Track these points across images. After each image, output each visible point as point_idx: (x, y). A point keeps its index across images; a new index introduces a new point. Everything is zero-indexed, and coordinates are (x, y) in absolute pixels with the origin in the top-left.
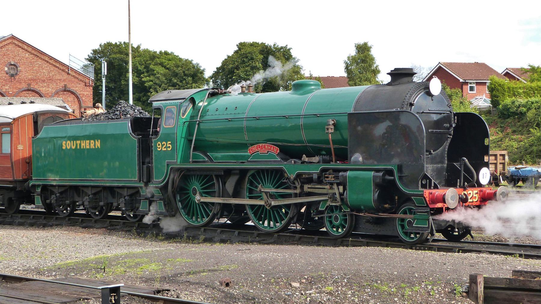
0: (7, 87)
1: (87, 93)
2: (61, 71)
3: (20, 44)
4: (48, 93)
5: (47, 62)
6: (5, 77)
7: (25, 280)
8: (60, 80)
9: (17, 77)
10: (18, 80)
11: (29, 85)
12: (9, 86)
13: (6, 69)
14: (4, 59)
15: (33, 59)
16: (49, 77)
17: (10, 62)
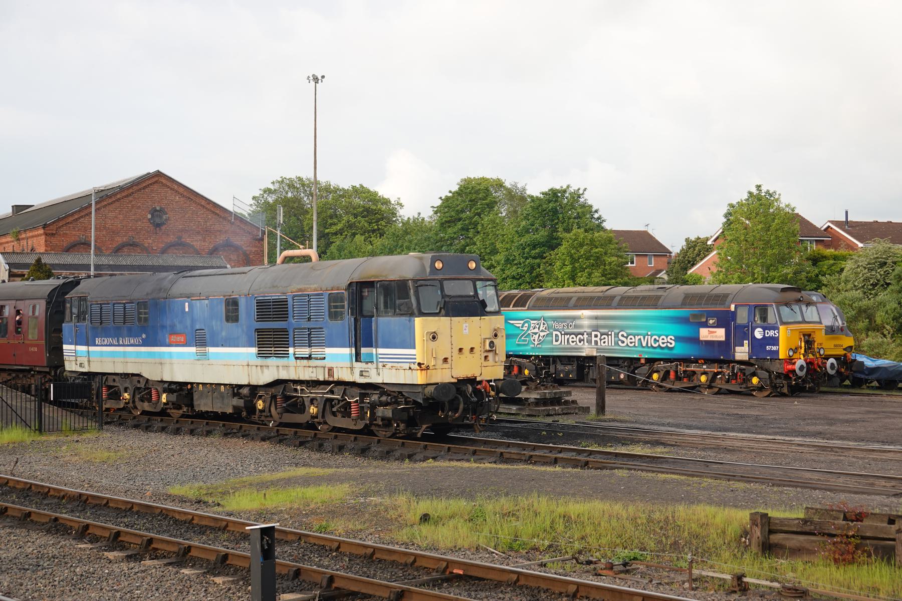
0: (150, 241)
1: (256, 249)
2: (221, 220)
3: (169, 184)
4: (204, 249)
5: (204, 207)
6: (148, 227)
7: (203, 405)
8: (220, 231)
9: (163, 228)
10: (165, 231)
11: (180, 238)
12: (153, 240)
13: (149, 216)
14: (148, 203)
15: (186, 203)
16: (206, 228)
17: (155, 208)
